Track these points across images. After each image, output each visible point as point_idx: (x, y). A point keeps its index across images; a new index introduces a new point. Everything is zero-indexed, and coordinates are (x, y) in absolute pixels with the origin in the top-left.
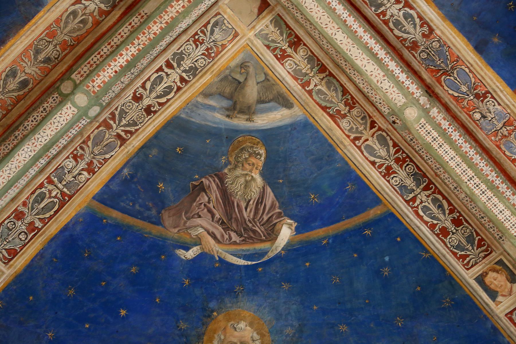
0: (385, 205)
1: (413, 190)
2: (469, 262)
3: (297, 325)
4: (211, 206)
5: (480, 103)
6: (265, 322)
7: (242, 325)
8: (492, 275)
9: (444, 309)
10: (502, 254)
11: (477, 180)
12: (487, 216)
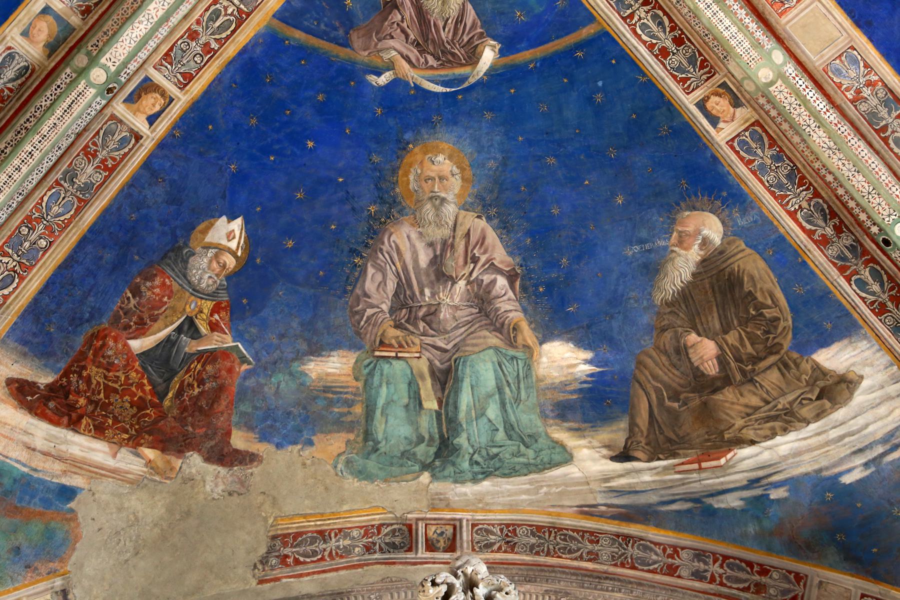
0: (600, 23)
1: (631, 6)
2: (689, 86)
3: (501, 158)
4: (405, 25)
6: (466, 155)
7: (441, 158)
8: (714, 99)
9: (661, 137)
10: (726, 75)
12: (711, 33)
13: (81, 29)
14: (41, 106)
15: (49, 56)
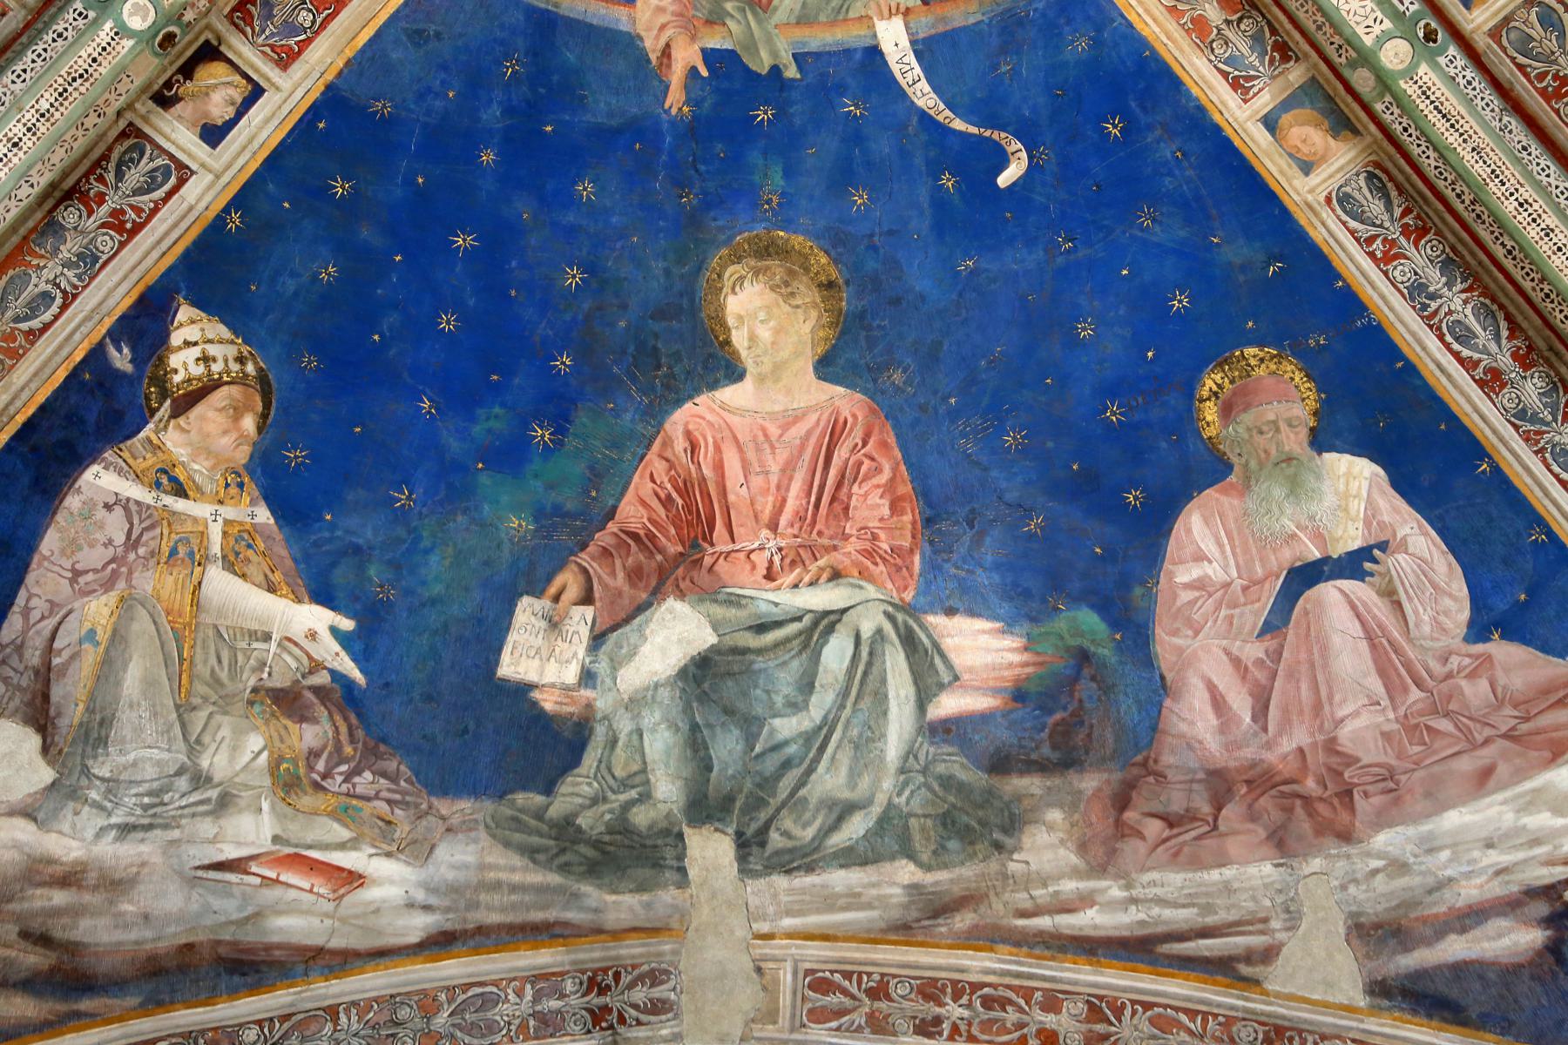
13: (1315, 66)
14: (1436, 168)
15: (1356, 132)
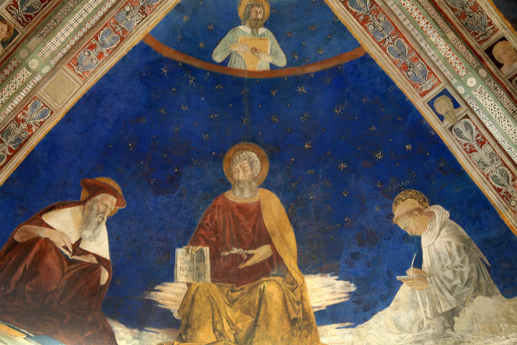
2: (12, 9)
5: (138, 10)
10: (23, 33)
11: (86, 16)
12: (58, 24)
